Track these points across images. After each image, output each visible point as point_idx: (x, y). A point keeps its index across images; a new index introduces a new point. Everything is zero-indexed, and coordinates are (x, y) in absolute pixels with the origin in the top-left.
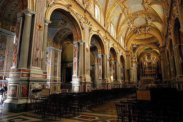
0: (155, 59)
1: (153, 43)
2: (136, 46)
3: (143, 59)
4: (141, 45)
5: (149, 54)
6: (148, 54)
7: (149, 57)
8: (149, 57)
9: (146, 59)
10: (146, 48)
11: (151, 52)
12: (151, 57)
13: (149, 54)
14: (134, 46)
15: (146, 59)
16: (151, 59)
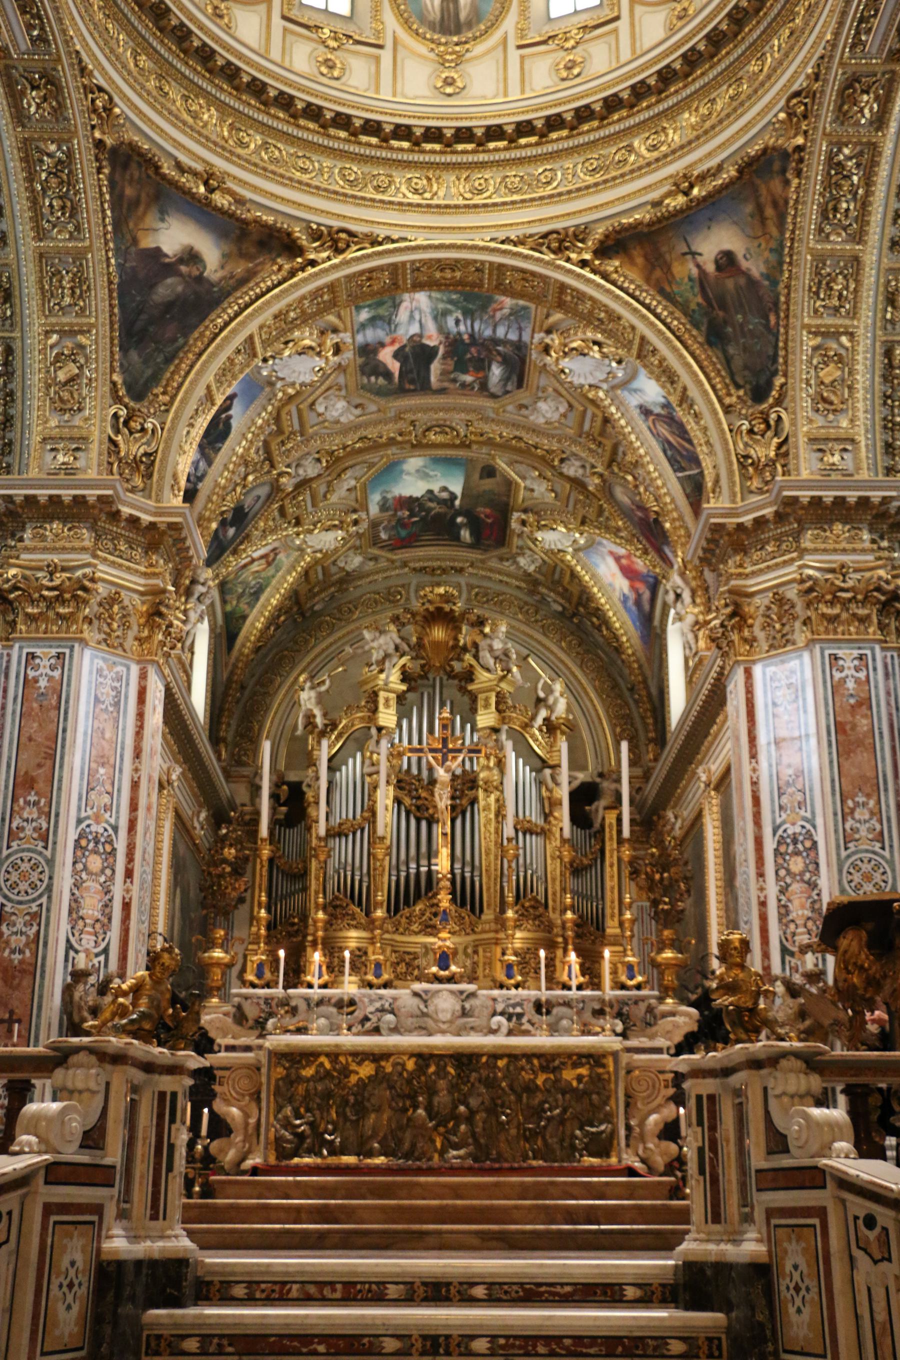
0: (550, 727)
1: (604, 250)
2: (211, 253)
3: (320, 700)
4: (336, 240)
5: (439, 633)
6: (439, 615)
7: (440, 677)
8: (440, 677)
9: (387, 717)
10: (416, 480)
11: (485, 597)
12: (483, 677)
13: (450, 620)
14: (173, 236)
15: (387, 717)
16: (486, 718)
